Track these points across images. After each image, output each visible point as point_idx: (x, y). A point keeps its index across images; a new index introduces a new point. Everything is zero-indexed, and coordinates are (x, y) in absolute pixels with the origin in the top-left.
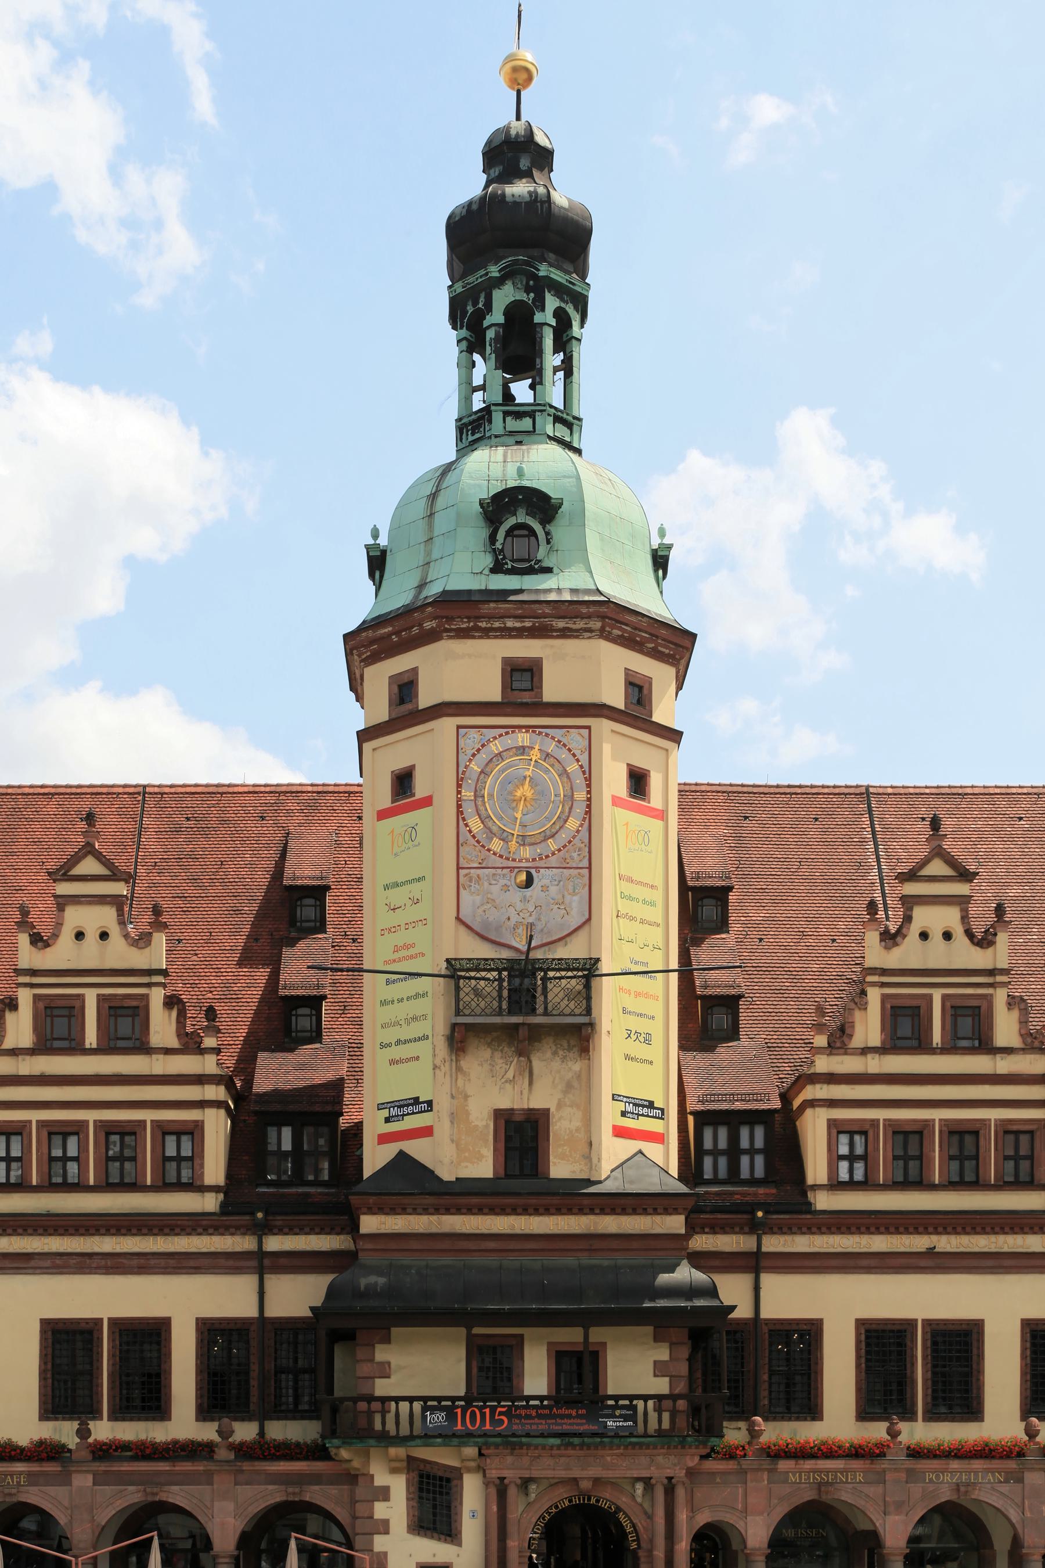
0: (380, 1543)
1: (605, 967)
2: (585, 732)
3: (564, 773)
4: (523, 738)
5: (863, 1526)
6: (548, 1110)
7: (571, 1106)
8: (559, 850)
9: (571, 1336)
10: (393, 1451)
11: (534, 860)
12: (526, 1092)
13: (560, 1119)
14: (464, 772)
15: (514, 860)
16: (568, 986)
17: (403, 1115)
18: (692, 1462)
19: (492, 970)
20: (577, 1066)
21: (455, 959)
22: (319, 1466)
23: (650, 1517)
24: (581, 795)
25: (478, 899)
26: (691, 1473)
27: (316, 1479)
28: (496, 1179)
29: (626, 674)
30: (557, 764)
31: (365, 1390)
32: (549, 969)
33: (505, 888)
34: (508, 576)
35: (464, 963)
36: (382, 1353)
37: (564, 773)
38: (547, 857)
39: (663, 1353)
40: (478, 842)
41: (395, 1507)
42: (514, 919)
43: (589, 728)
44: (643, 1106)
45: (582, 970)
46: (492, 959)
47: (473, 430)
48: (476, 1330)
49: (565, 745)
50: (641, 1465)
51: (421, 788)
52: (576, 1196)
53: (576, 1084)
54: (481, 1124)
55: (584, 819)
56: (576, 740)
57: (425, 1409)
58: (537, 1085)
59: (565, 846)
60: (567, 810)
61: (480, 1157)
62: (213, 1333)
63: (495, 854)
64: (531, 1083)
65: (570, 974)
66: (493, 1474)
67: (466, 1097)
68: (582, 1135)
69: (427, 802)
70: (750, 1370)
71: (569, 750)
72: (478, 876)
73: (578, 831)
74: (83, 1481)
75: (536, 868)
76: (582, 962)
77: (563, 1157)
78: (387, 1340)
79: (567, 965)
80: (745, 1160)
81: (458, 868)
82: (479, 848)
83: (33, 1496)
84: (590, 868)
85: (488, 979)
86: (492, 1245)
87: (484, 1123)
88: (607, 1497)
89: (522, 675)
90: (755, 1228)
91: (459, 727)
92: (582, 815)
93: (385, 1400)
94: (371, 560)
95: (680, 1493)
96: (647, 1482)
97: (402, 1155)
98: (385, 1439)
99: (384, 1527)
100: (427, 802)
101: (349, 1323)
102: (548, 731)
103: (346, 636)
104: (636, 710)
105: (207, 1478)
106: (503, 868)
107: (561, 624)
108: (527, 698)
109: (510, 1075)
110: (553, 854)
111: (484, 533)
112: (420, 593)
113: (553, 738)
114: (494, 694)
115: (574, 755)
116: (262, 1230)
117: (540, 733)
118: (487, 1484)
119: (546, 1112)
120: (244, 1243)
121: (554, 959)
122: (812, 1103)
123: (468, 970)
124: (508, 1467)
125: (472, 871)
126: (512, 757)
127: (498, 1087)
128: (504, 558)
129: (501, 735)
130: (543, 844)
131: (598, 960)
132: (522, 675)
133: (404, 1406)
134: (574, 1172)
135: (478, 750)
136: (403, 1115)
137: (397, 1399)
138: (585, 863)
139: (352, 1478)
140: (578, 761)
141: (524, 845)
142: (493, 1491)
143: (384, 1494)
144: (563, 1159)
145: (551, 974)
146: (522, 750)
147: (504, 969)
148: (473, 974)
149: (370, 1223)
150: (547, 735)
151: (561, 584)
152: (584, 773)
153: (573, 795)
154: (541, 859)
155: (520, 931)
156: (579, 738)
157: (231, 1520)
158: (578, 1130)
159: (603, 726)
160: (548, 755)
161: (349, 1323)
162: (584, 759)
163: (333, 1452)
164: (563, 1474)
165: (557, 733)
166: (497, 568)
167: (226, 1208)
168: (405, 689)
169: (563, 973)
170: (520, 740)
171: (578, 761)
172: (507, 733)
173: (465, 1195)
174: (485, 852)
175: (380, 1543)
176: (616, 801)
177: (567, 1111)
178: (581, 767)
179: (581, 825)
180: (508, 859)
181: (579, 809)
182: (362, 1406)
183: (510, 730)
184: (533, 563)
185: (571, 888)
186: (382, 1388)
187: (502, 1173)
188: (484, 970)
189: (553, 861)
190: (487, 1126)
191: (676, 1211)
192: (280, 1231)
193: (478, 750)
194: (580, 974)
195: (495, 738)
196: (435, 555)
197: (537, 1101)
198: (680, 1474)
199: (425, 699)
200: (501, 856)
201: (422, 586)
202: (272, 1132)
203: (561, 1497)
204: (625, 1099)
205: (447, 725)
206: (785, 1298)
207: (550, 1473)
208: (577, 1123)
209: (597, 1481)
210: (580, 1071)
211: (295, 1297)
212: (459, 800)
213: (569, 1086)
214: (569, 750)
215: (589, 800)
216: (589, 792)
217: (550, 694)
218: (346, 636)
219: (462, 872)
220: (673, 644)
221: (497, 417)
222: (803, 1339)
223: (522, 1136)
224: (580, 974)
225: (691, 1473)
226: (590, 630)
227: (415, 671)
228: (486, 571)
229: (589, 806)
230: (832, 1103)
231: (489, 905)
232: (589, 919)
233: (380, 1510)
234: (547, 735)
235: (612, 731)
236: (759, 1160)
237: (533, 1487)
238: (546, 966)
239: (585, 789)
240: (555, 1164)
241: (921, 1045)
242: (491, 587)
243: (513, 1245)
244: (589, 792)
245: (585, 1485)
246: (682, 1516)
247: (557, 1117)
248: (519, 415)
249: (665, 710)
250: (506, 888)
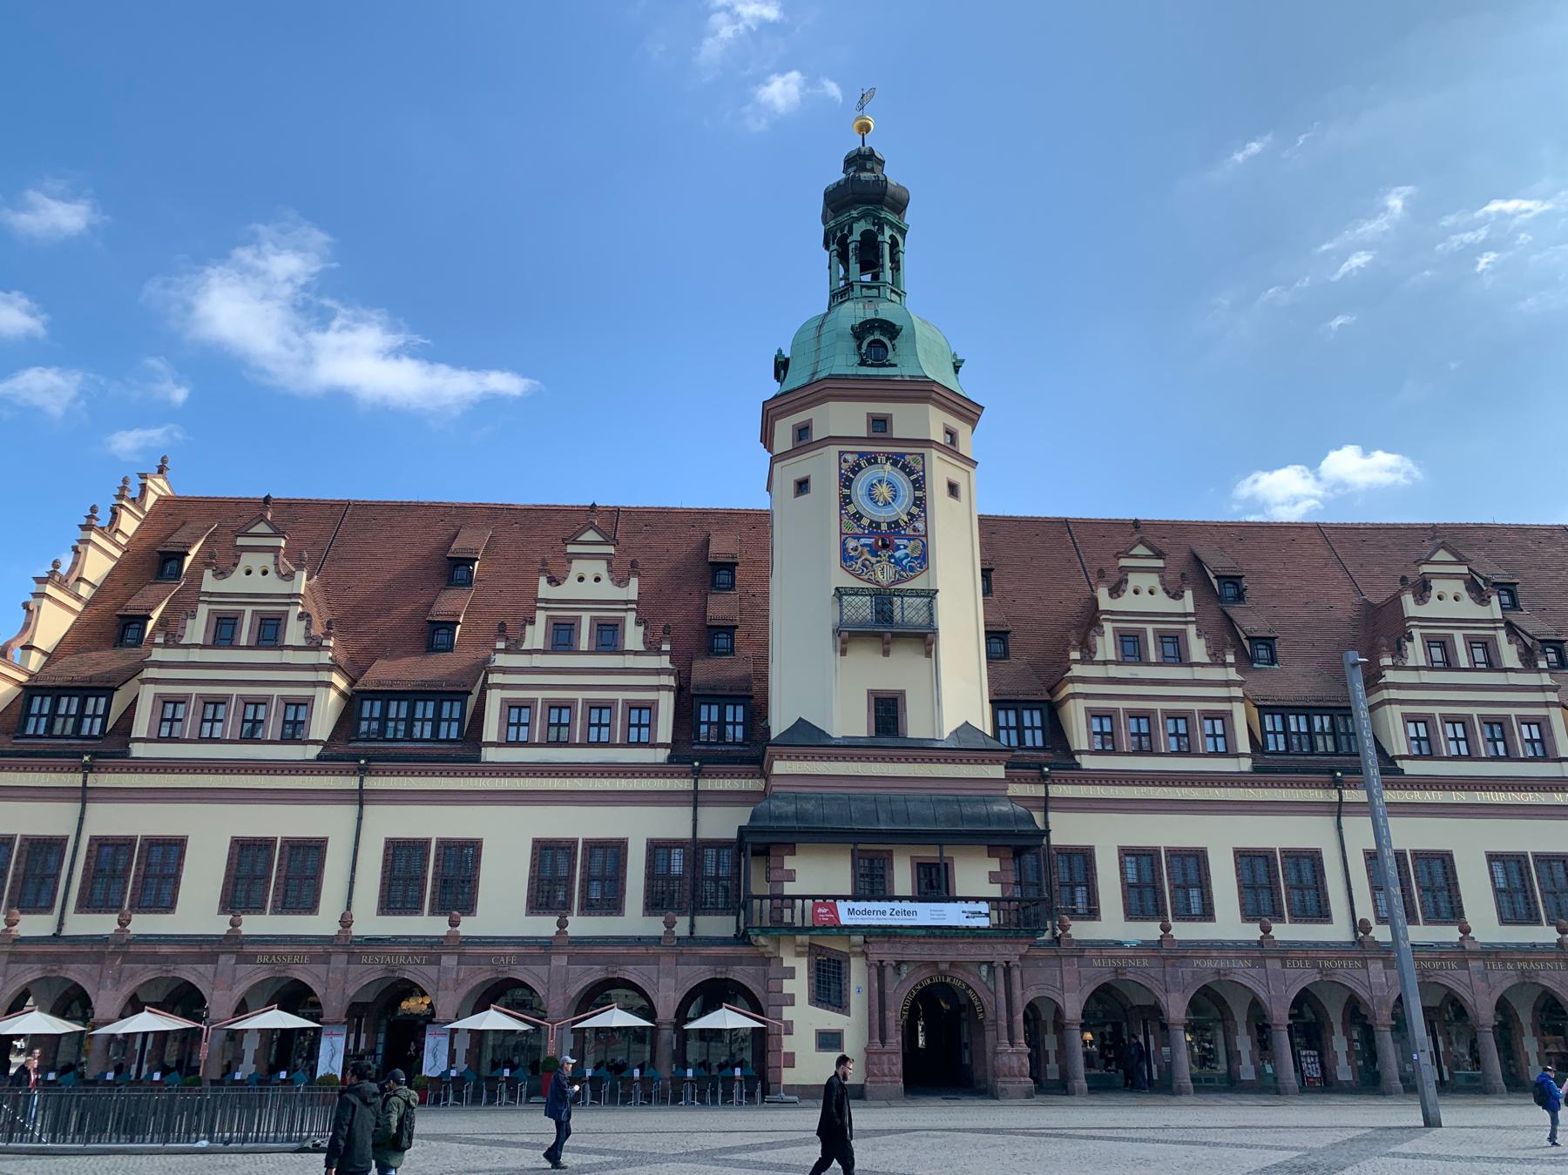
0: (788, 1013)
5: (1139, 1000)
9: (930, 853)
10: (799, 938)
18: (1023, 949)
22: (742, 950)
23: (995, 993)
26: (1022, 957)
27: (739, 960)
31: (777, 892)
36: (790, 863)
39: (994, 865)
41: (799, 985)
47: (839, 296)
48: (860, 847)
50: (984, 952)
52: (925, 750)
57: (816, 906)
62: (657, 848)
66: (874, 958)
70: (1045, 883)
74: (560, 961)
78: (793, 853)
80: (1028, 733)
83: (520, 974)
88: (960, 978)
90: (1043, 779)
93: (793, 898)
95: (1016, 973)
96: (990, 964)
98: (792, 930)
99: (790, 1000)
101: (766, 842)
104: (951, 445)
105: (656, 959)
111: (853, 344)
114: (863, 432)
116: (697, 774)
118: (869, 967)
120: (685, 784)
122: (1074, 696)
124: (885, 952)
133: (809, 902)
137: (803, 898)
139: (766, 960)
142: (874, 971)
143: (791, 973)
149: (779, 767)
151: (904, 370)
157: (672, 994)
161: (766, 842)
163: (753, 938)
164: (927, 958)
167: (671, 759)
173: (849, 749)
175: (788, 1013)
182: (777, 902)
186: (789, 889)
191: (998, 762)
192: (710, 776)
198: (1015, 960)
199: (816, 435)
202: (704, 708)
203: (924, 977)
205: (834, 450)
206: (1065, 830)
207: (917, 958)
209: (952, 964)
211: (722, 823)
217: (898, 432)
220: (969, 412)
221: (857, 288)
222: (1084, 857)
223: (887, 710)
225: (1022, 957)
230: (1086, 696)
233: (788, 986)
236: (1038, 733)
237: (904, 968)
241: (1141, 660)
245: (944, 967)
246: (1017, 992)
248: (869, 288)
249: (964, 447)
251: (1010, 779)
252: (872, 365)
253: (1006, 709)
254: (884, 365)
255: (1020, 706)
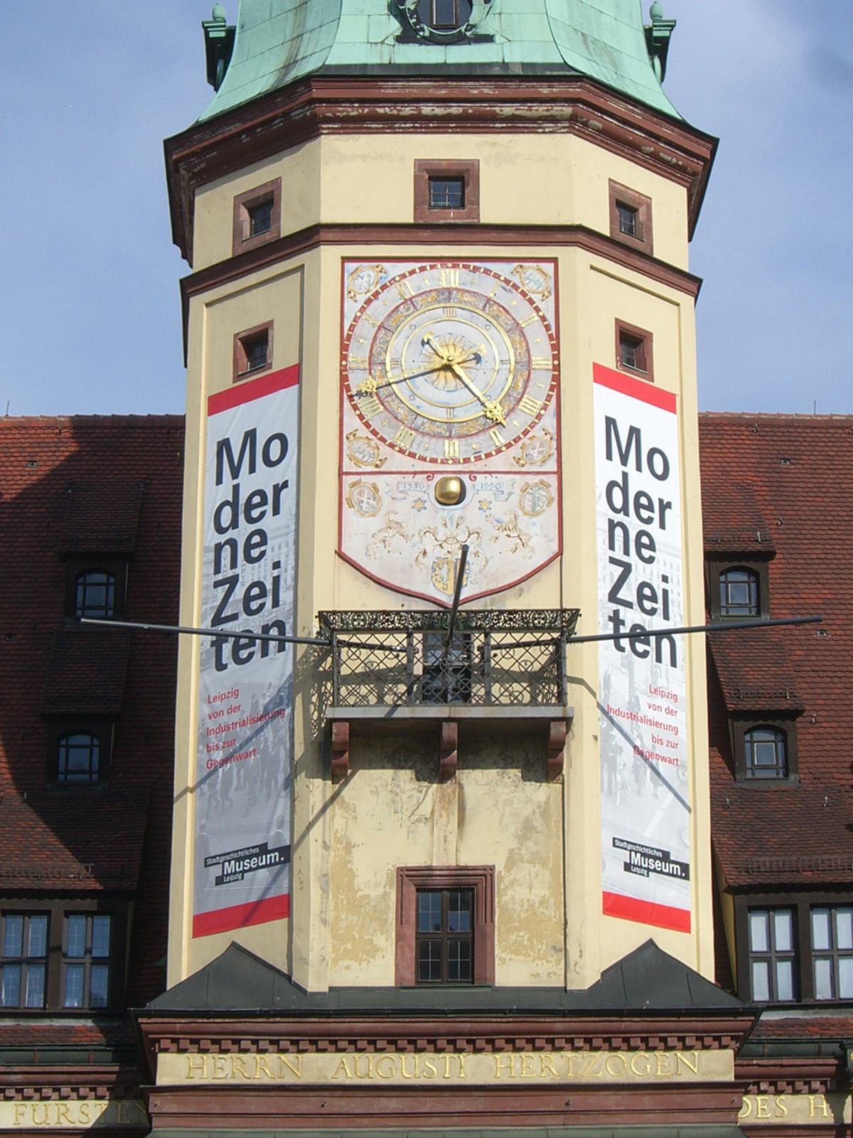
1: (582, 628)
2: (549, 267)
3: (516, 329)
4: (451, 277)
6: (492, 868)
7: (531, 862)
8: (509, 446)
11: (466, 461)
12: (453, 839)
13: (512, 884)
14: (352, 328)
15: (433, 461)
16: (527, 657)
17: (244, 872)
19: (397, 630)
20: (541, 792)
21: (334, 613)
24: (542, 358)
25: (374, 523)
28: (400, 987)
29: (612, 189)
30: (503, 315)
32: (493, 629)
33: (419, 505)
34: (423, 47)
35: (349, 618)
37: (516, 329)
38: (488, 455)
40: (374, 433)
42: (435, 553)
43: (554, 260)
44: (656, 858)
45: (550, 629)
46: (398, 613)
49: (515, 287)
51: (281, 356)
53: (538, 823)
54: (375, 893)
55: (549, 398)
56: (535, 279)
58: (468, 828)
59: (517, 440)
60: (521, 384)
61: (373, 951)
63: (402, 451)
64: (461, 823)
65: (529, 637)
67: (349, 847)
68: (552, 913)
69: (292, 376)
71: (524, 294)
72: (375, 487)
73: (539, 417)
75: (471, 472)
76: (549, 616)
77: (518, 949)
79: (525, 621)
81: (341, 474)
82: (375, 441)
84: (559, 473)
85: (390, 649)
86: (391, 1104)
87: (380, 891)
89: (449, 184)
91: (345, 259)
92: (546, 392)
94: (210, 43)
97: (234, 946)
100: (292, 376)
102: (489, 265)
103: (167, 143)
106: (415, 473)
107: (508, 110)
108: (452, 216)
109: (426, 809)
110: (499, 451)
112: (286, 74)
113: (497, 276)
115: (531, 301)
117: (476, 269)
119: (487, 874)
121: (501, 612)
123: (357, 630)
125: (364, 478)
126: (430, 303)
127: (405, 829)
128: (419, 22)
129: (412, 272)
130: (481, 437)
131: (576, 614)
132: (449, 184)
134: (538, 975)
135: (376, 295)
136: (244, 872)
138: (552, 466)
140: (537, 309)
141: (450, 437)
144: (516, 953)
145: (497, 637)
146: (446, 294)
147: (417, 629)
148: (363, 638)
150: (487, 272)
152: (547, 328)
153: (529, 361)
154: (478, 459)
155: (444, 572)
156: (538, 276)
158: (543, 902)
159: (576, 259)
160: (489, 300)
162: (548, 308)
165: (503, 269)
166: (407, 36)
168: (262, 207)
169: (518, 636)
170: (443, 279)
171: (537, 309)
172: (422, 269)
174: (384, 449)
176: (602, 375)
177: (525, 871)
178: (543, 319)
179: (545, 407)
180: (424, 459)
181: (542, 382)
183: (428, 265)
184: (463, 28)
185: (528, 505)
187: (410, 977)
188: (384, 630)
189: (497, 463)
190: (385, 895)
193: (376, 295)
194: (546, 637)
195: (403, 276)
196: (310, 25)
197: (472, 856)
200: (412, 455)
201: (288, 67)
204: (630, 847)
208: (541, 891)
210: (547, 802)
212: (343, 369)
213: (527, 830)
214: (524, 294)
215: (557, 368)
216: (556, 357)
217: (490, 213)
218: (167, 143)
219: (348, 480)
223: (448, 916)
224: (546, 637)
226: (553, 119)
227: (277, 183)
228: (391, 41)
229: (557, 379)
231: (391, 532)
232: (560, 553)
234: (487, 272)
235: (592, 268)
238: (489, 621)
239: (549, 353)
240: (503, 961)
242: (399, 60)
243: (428, 1104)
244: (556, 357)
247: (506, 881)
250: (420, 505)
251: (743, 1084)
252: (431, 41)
253: (769, 909)
254: (461, 40)
255: (802, 898)
